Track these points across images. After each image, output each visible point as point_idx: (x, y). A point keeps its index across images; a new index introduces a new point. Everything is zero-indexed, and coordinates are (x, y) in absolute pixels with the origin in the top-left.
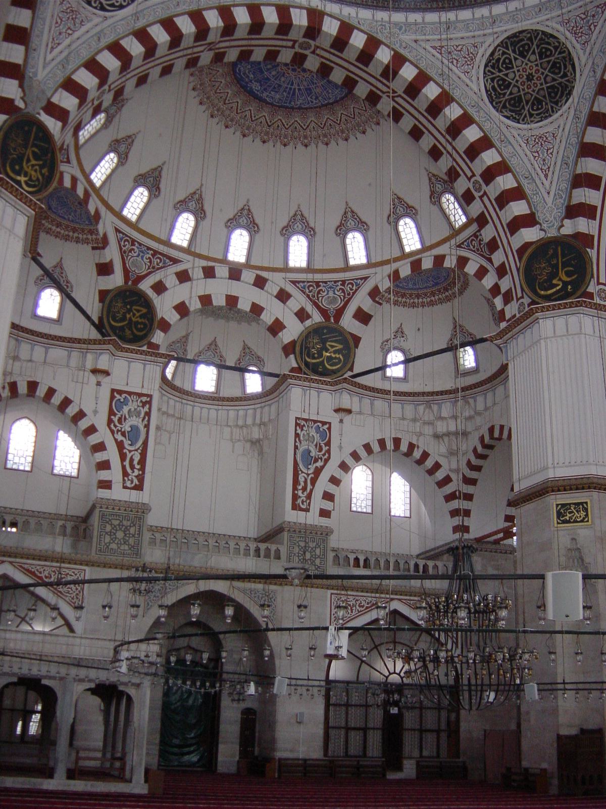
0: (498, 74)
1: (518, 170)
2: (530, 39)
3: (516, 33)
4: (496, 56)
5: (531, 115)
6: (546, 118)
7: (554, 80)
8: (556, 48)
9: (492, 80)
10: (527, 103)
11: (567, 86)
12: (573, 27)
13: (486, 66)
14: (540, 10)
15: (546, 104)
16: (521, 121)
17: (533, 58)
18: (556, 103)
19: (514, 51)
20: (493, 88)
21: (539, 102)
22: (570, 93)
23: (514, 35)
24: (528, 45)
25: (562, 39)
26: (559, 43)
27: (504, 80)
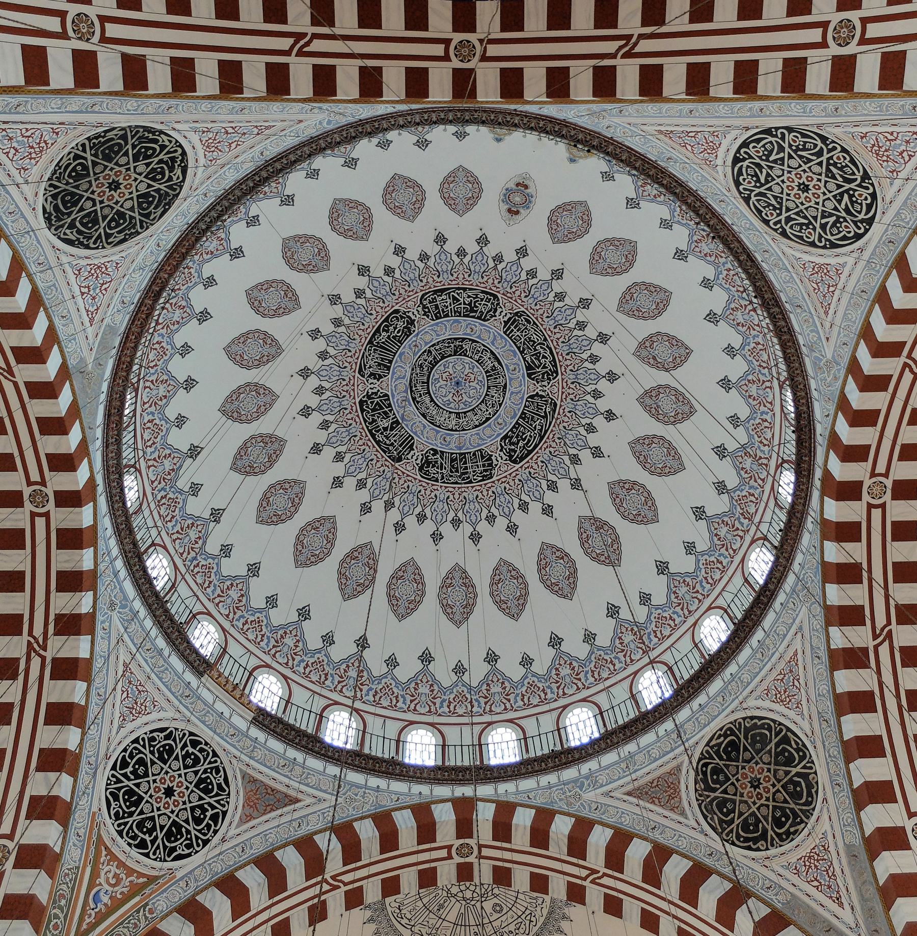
0: (161, 157)
1: (40, 101)
2: (147, 216)
3: (170, 207)
4: (178, 172)
5: (77, 157)
6: (55, 172)
7: (81, 209)
8: (108, 236)
9: (163, 147)
10: (95, 164)
11: (59, 219)
12: (107, 269)
13: (184, 153)
14: (158, 245)
15: (67, 183)
16: (87, 142)
17: (128, 204)
18: (54, 197)
19: (158, 191)
20: (155, 141)
21: (78, 177)
22: (48, 219)
23: (170, 204)
24: (144, 209)
25: (109, 250)
26: (109, 244)
27: (146, 157)
